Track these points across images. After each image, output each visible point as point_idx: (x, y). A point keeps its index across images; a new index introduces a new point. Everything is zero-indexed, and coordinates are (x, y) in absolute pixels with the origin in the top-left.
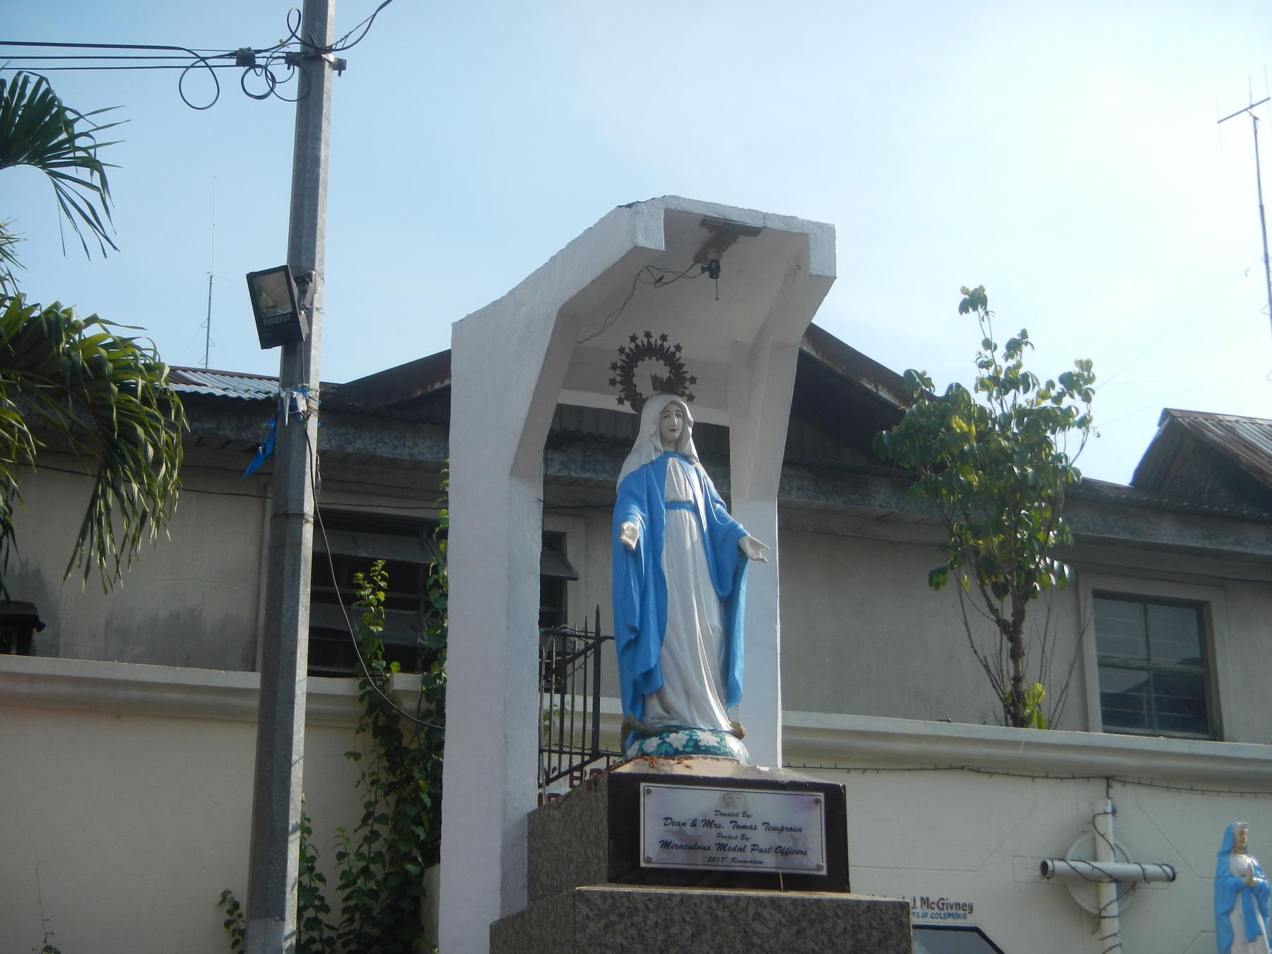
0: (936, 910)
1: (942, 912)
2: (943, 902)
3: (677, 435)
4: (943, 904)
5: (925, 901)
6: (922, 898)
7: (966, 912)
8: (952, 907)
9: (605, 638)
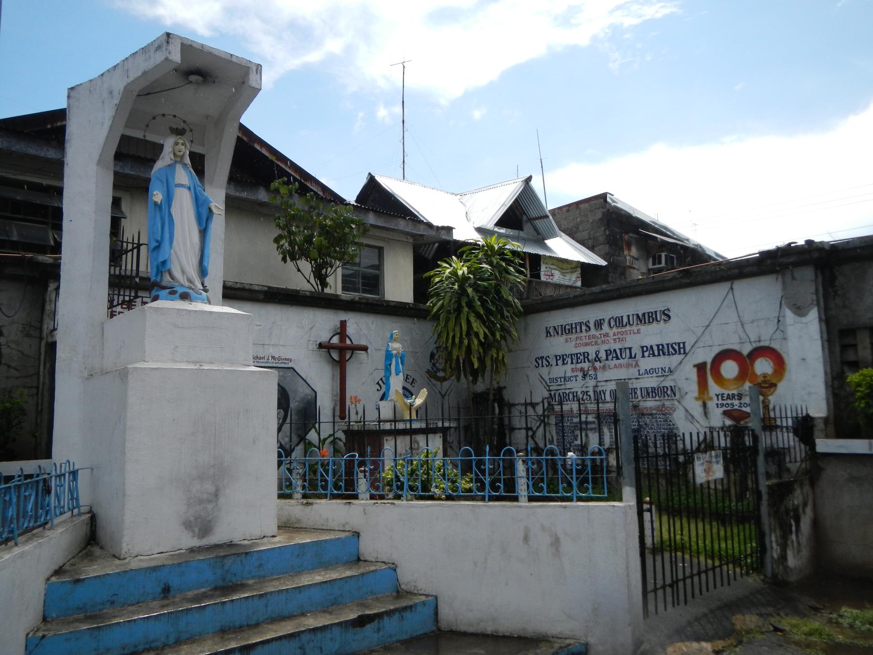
0: (277, 361)
3: (181, 154)
5: (273, 357)
9: (142, 245)
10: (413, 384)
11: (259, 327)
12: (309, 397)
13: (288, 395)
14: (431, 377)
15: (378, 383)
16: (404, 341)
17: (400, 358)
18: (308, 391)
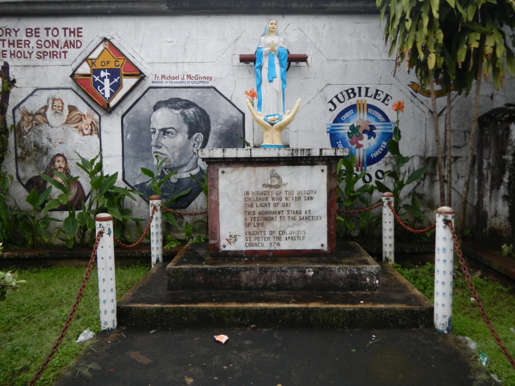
0: (194, 80)
1: (197, 81)
4: (198, 77)
5: (189, 76)
6: (187, 75)
8: (201, 79)
10: (386, 102)
11: (170, 44)
12: (235, 119)
13: (208, 117)
14: (416, 92)
15: (331, 102)
16: (373, 47)
17: (278, 56)
18: (234, 112)
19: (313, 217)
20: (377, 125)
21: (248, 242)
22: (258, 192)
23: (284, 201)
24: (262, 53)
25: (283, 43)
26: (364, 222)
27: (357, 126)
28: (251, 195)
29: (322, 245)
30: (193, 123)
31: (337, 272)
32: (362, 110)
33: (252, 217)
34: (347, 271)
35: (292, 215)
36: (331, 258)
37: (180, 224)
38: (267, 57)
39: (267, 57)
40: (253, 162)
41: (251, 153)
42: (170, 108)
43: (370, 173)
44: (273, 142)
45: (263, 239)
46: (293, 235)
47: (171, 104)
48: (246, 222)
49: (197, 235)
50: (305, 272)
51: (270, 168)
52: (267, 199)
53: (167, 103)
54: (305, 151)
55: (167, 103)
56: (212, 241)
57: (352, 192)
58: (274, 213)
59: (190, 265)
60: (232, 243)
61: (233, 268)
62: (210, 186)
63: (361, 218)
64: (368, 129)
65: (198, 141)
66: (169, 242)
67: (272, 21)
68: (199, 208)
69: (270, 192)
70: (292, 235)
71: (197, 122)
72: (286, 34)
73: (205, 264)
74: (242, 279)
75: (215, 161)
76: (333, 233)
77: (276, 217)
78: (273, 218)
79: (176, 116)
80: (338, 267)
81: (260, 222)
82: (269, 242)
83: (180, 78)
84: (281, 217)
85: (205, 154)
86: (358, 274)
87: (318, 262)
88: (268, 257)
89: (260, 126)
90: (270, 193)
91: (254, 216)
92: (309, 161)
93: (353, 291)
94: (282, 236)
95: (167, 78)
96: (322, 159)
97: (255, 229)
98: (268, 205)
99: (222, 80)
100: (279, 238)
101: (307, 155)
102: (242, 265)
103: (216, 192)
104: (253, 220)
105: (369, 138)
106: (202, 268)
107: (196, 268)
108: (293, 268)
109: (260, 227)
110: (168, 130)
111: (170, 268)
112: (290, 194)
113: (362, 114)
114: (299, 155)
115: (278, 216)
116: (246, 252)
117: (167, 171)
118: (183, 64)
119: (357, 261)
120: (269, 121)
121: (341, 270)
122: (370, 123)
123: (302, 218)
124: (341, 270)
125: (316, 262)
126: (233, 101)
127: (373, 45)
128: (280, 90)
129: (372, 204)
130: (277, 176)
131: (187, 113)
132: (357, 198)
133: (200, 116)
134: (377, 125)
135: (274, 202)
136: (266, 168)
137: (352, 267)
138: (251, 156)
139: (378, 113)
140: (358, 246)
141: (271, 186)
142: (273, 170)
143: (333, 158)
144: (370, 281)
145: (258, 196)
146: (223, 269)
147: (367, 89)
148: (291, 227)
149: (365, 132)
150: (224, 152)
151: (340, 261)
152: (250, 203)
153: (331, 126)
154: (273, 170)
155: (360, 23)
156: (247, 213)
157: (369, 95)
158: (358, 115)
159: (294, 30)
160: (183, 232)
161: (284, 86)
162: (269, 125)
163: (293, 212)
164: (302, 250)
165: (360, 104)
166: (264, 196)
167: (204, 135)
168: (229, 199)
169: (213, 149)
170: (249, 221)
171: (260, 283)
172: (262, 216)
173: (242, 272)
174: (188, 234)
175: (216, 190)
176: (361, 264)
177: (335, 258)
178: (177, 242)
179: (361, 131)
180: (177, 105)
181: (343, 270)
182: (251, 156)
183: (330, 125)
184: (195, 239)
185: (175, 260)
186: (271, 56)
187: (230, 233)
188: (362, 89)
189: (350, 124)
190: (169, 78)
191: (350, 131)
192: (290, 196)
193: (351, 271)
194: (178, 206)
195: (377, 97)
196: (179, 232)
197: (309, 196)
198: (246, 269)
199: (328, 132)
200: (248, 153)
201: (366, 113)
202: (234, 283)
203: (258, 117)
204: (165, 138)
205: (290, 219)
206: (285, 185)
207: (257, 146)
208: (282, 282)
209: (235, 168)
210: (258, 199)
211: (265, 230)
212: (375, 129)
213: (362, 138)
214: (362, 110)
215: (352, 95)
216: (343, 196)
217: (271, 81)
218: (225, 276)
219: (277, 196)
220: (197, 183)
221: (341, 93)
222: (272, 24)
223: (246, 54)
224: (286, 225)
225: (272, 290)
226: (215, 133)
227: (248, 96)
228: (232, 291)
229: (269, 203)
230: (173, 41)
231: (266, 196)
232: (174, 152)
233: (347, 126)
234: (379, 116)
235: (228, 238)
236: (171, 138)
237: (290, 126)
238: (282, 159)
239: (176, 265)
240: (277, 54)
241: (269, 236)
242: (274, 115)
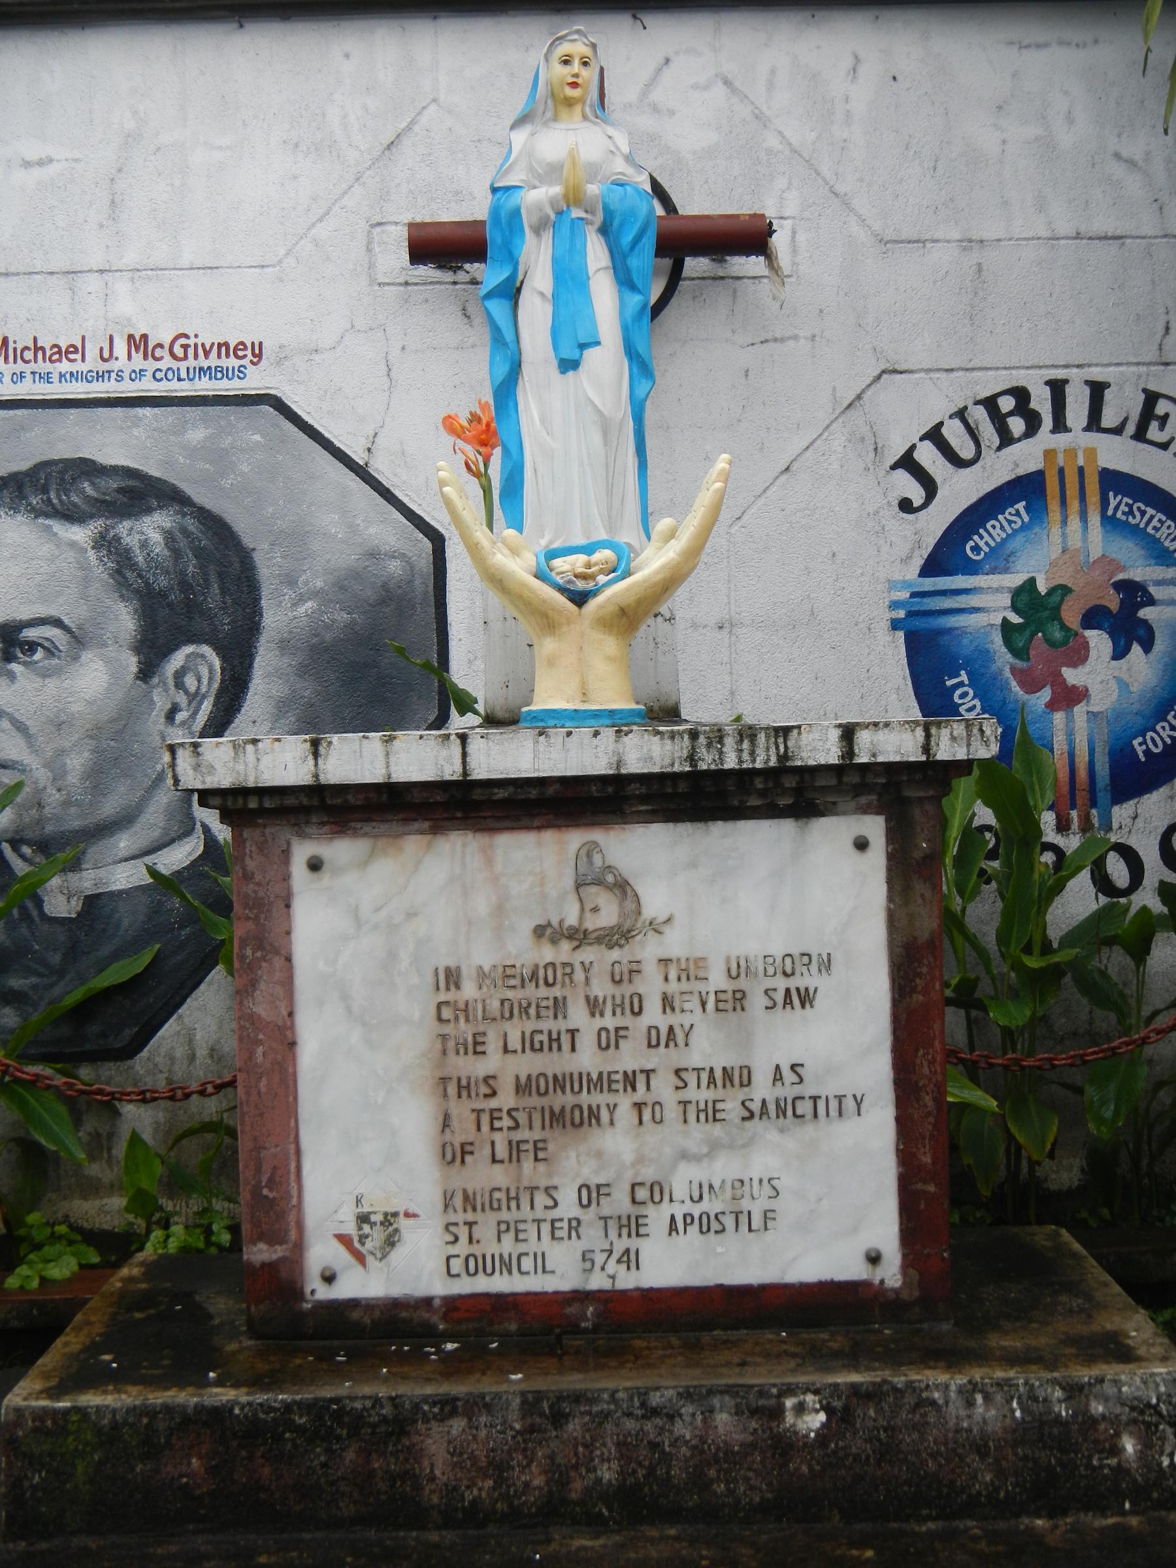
0: (167, 362)
1: (183, 365)
2: (183, 341)
4: (185, 347)
5: (139, 343)
6: (131, 337)
7: (245, 362)
8: (207, 354)
11: (36, 173)
12: (395, 567)
13: (245, 558)
15: (908, 462)
16: (1118, 170)
17: (604, 230)
19: (815, 1099)
20: (1158, 583)
21: (462, 1248)
22: (507, 973)
23: (653, 1015)
24: (516, 213)
25: (629, 159)
26: (1108, 1114)
27: (1051, 592)
28: (469, 990)
29: (874, 1259)
30: (163, 594)
31: (955, 1410)
32: (1074, 505)
33: (478, 1112)
34: (1009, 1401)
35: (704, 1095)
36: (925, 1326)
37: (99, 1146)
38: (547, 236)
39: (547, 236)
40: (478, 805)
41: (464, 755)
42: (38, 513)
43: (1133, 842)
44: (585, 696)
45: (546, 1228)
46: (710, 1205)
47: (45, 490)
48: (448, 1136)
49: (195, 1204)
50: (777, 1413)
51: (575, 839)
52: (559, 1007)
53: (20, 487)
54: (762, 738)
55: (20, 487)
56: (262, 1246)
57: (1037, 949)
58: (603, 1082)
59: (134, 1390)
60: (370, 1259)
61: (377, 1401)
62: (244, 943)
63: (1090, 1091)
64: (1113, 602)
65: (192, 689)
66: (38, 1247)
67: (564, 48)
68: (202, 1052)
69: (578, 967)
70: (705, 1206)
71: (185, 585)
72: (655, 109)
73: (219, 1383)
74: (426, 1463)
75: (267, 804)
76: (931, 1188)
77: (612, 1109)
78: (594, 1114)
79: (71, 555)
80: (961, 1380)
81: (522, 1134)
82: (576, 1247)
83: (92, 352)
84: (639, 1106)
85: (211, 769)
86: (1075, 1415)
87: (852, 1358)
88: (573, 1328)
89: (512, 611)
90: (579, 976)
91: (493, 1103)
92: (785, 792)
93: (1051, 1516)
94: (650, 1211)
95: (20, 356)
96: (854, 779)
97: (500, 1176)
98: (565, 1039)
99: (316, 357)
100: (634, 1226)
101: (773, 762)
102: (428, 1380)
103: (278, 976)
104: (485, 1127)
105: (1119, 653)
106: (199, 1408)
107: (168, 1409)
108: (711, 1392)
109: (528, 1164)
110: (31, 634)
111: (18, 1411)
112: (686, 974)
113: (1074, 522)
114: (731, 763)
115: (625, 1103)
116: (453, 1304)
117: (23, 857)
118: (106, 276)
119: (1070, 1341)
120: (560, 580)
121: (979, 1398)
122: (1123, 569)
123: (755, 1106)
124: (979, 1398)
125: (836, 1354)
126: (382, 470)
127: (1117, 156)
128: (622, 412)
129: (1146, 1011)
130: (610, 878)
131: (131, 541)
132: (1068, 979)
133: (199, 553)
134: (1158, 583)
135: (598, 1022)
136: (549, 836)
137: (1038, 1376)
138: (465, 773)
139: (1160, 516)
140: (1075, 1255)
141: (579, 937)
142: (591, 849)
143: (918, 776)
144: (1141, 1455)
145: (510, 994)
146: (316, 1408)
147: (1097, 390)
148: (697, 1158)
149: (1093, 617)
150: (316, 755)
151: (972, 1344)
152: (465, 1030)
153: (914, 595)
154: (591, 849)
155: (1046, 45)
156: (452, 1089)
157: (1109, 418)
158: (1056, 530)
159: (695, 87)
160: (114, 1188)
161: (641, 392)
162: (561, 600)
163: (704, 1076)
164: (764, 1289)
165: (1061, 471)
166: (543, 991)
167: (224, 658)
168: (349, 1010)
169: (255, 742)
170: (463, 1130)
171: (527, 1485)
172: (535, 1101)
173: (426, 1420)
174: (142, 1202)
175: (278, 962)
176: (1090, 1360)
177: (946, 1327)
178: (83, 1247)
179: (1071, 615)
180: (75, 498)
181: (987, 1398)
182: (465, 773)
183: (906, 584)
184: (177, 1229)
185: (50, 1359)
186: (565, 230)
187: (358, 1201)
188: (1069, 390)
189: (1015, 580)
190: (28, 355)
191: (1016, 619)
192: (685, 986)
193: (1035, 1399)
194: (88, 1047)
195: (1153, 432)
196: (91, 1188)
197: (793, 983)
198: (448, 1407)
199: (895, 625)
200: (449, 760)
201: (1095, 519)
202: (382, 1486)
203: (502, 559)
204: (12, 676)
205: (692, 1117)
206: (656, 927)
207: (500, 714)
208: (651, 1471)
209: (381, 842)
210: (509, 1011)
211: (555, 1181)
212: (1151, 602)
213: (1079, 655)
214: (1074, 505)
215: (1017, 425)
216: (988, 971)
217: (568, 365)
218: (329, 1451)
219: (617, 991)
220: (191, 917)
221: (961, 414)
222: (566, 63)
223: (445, 217)
224: (668, 1150)
225: (594, 1523)
226: (284, 645)
227: (460, 443)
228: (372, 1534)
229: (573, 1032)
230: (51, 160)
231: (557, 991)
232: (61, 753)
233: (998, 590)
234: (1164, 531)
235: (350, 1229)
236: (45, 675)
237: (678, 602)
238: (635, 789)
239: (55, 1393)
240: (599, 219)
241: (576, 1212)
242: (589, 550)
